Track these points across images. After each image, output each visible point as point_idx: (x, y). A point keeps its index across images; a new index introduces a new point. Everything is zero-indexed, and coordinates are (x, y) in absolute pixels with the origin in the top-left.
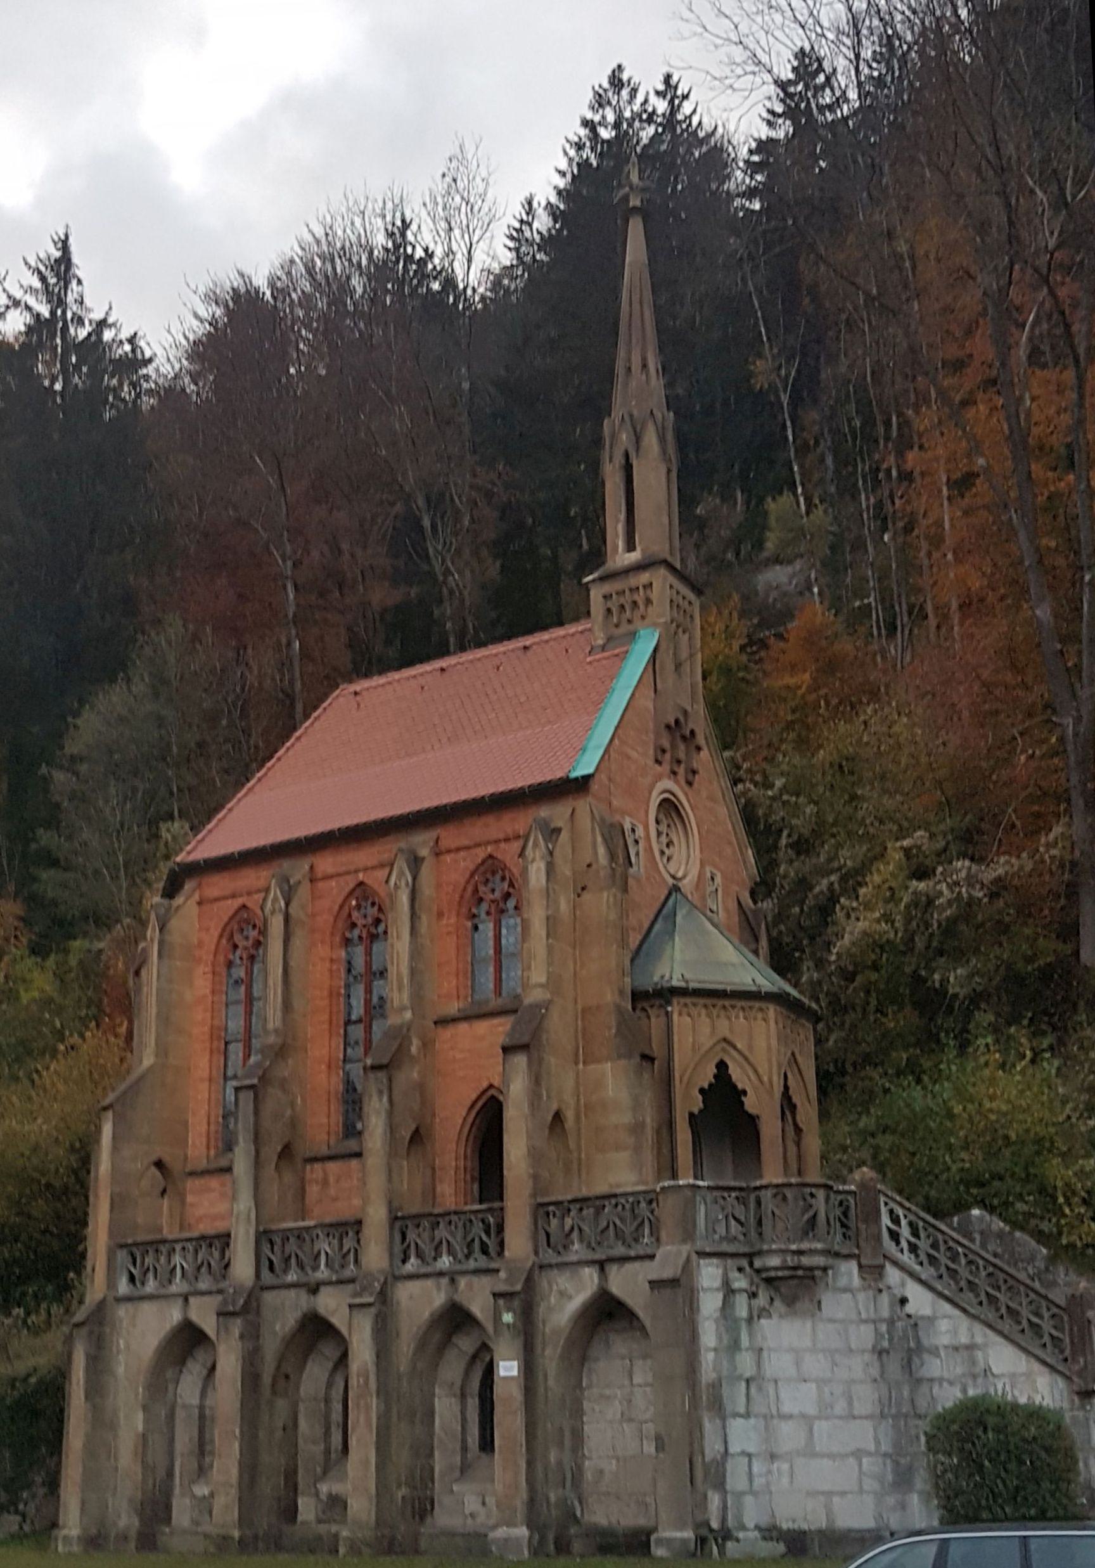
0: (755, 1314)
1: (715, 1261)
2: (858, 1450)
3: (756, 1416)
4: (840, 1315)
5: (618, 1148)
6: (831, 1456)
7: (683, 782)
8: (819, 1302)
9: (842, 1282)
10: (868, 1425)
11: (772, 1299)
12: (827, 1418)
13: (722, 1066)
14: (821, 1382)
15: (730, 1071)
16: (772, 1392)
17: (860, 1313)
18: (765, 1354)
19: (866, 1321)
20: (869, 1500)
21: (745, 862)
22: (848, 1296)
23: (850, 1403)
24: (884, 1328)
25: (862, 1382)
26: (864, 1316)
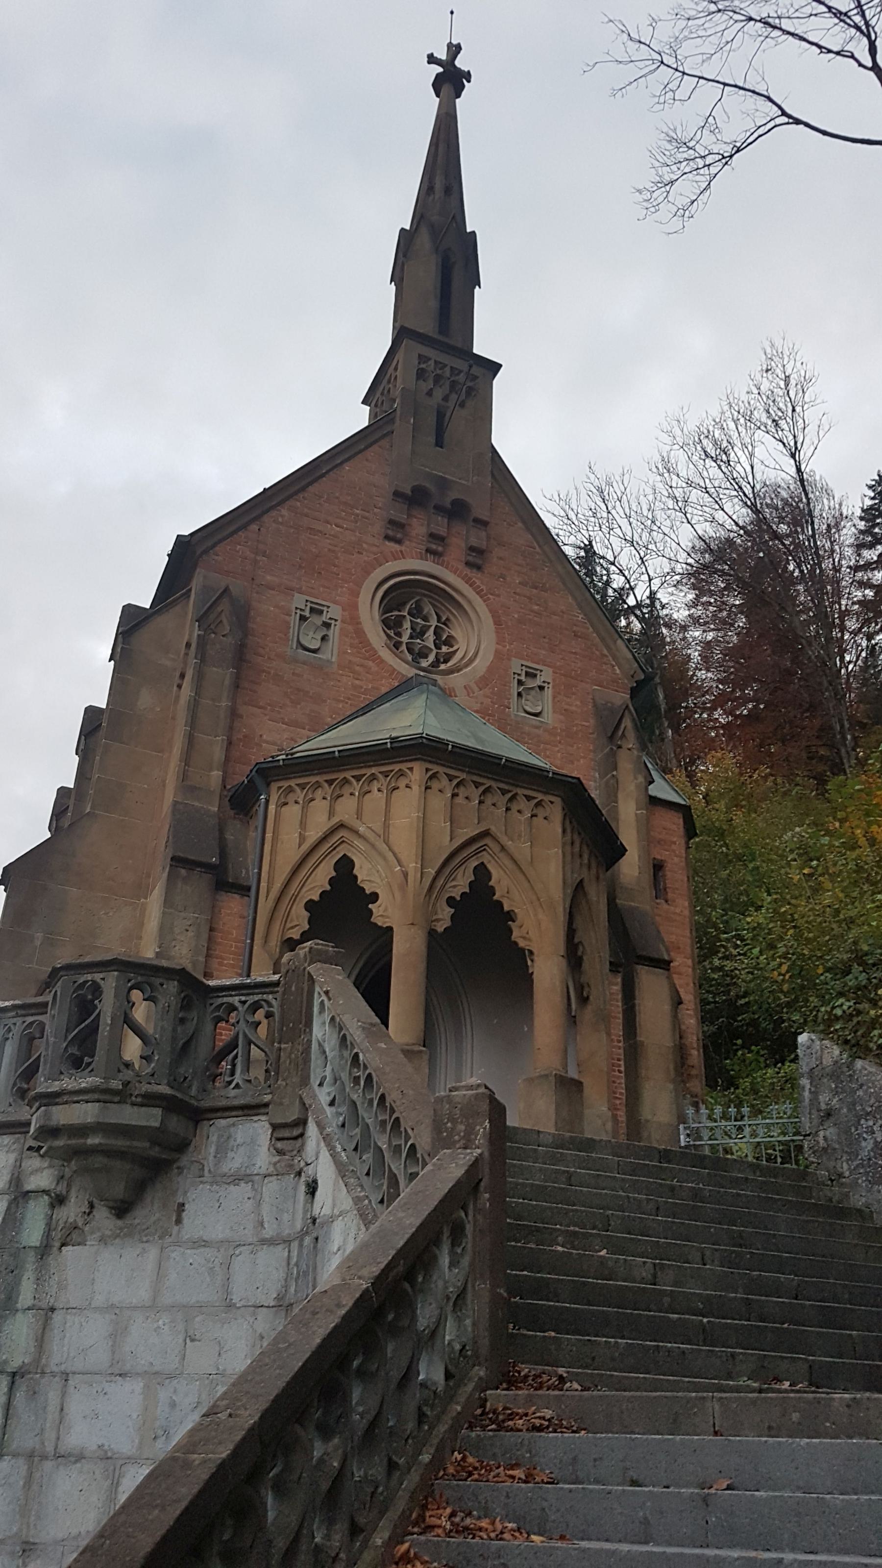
0: (57, 1235)
3: (15, 1455)
4: (218, 1231)
9: (234, 1163)
11: (92, 1206)
13: (345, 866)
15: (355, 872)
16: (53, 1397)
17: (262, 1224)
18: (57, 1317)
19: (270, 1242)
21: (614, 658)
22: (245, 1189)
26: (269, 1231)
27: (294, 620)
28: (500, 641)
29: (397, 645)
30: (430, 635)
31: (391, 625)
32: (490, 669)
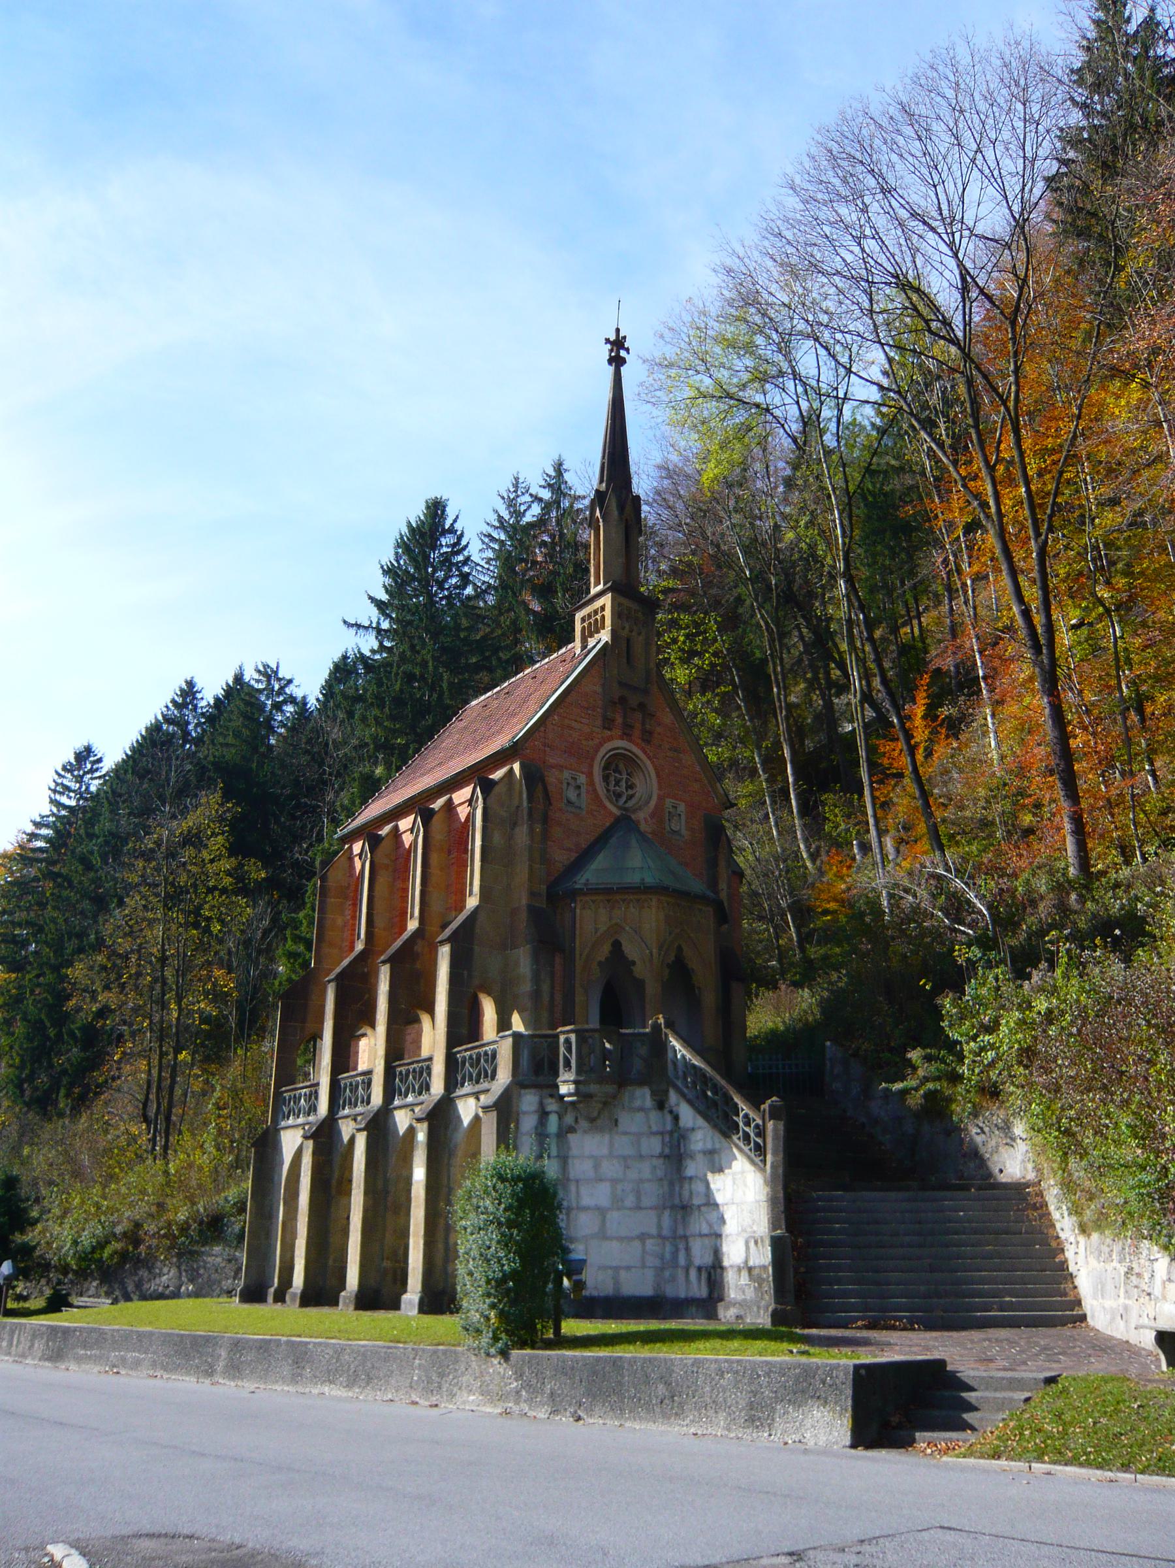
1: (533, 1091)
2: (643, 1234)
4: (634, 1129)
6: (620, 1239)
7: (639, 741)
8: (616, 1121)
9: (638, 1103)
10: (653, 1214)
12: (618, 1209)
13: (617, 945)
14: (614, 1182)
15: (624, 948)
17: (650, 1127)
18: (570, 1161)
20: (650, 1274)
23: (639, 1198)
24: (667, 1139)
25: (649, 1180)
26: (654, 1129)
27: (565, 785)
28: (660, 788)
29: (608, 790)
30: (623, 784)
31: (606, 778)
32: (656, 806)
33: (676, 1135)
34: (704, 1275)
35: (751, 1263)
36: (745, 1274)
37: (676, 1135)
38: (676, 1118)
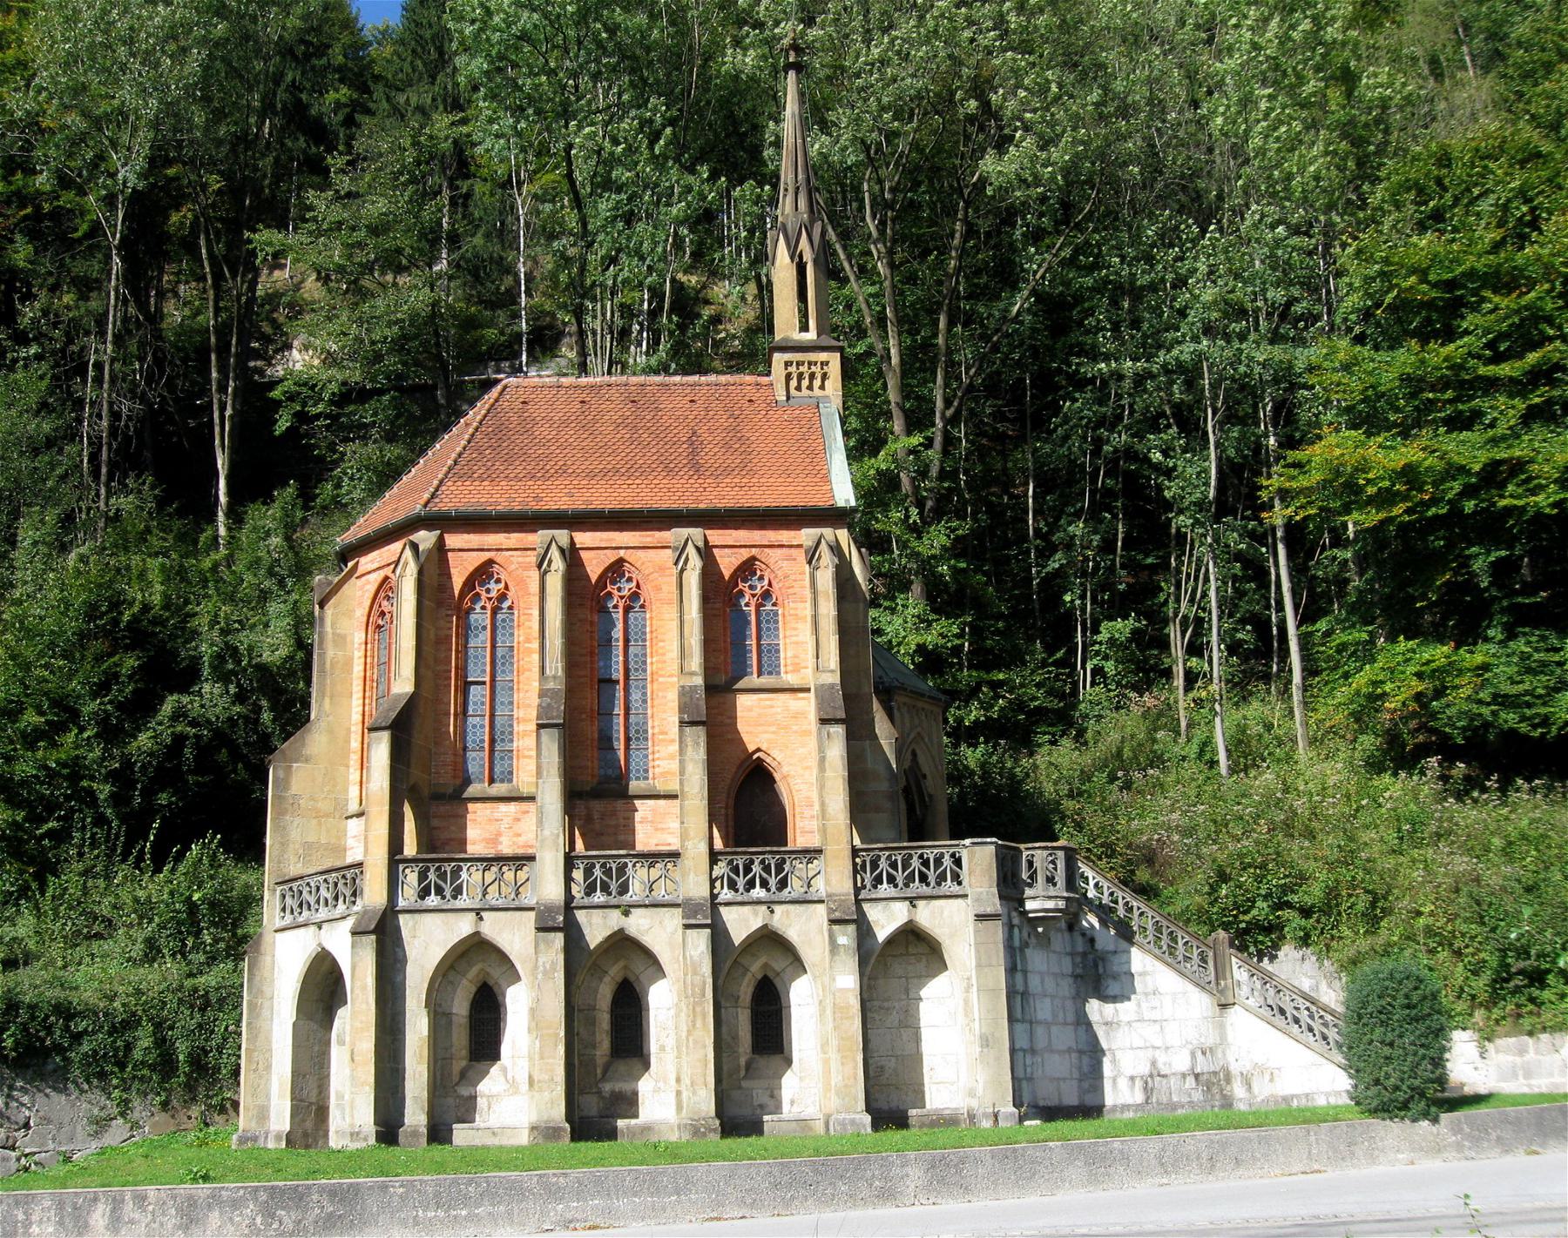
5: (878, 810)
24: (1078, 959)
33: (1091, 957)
34: (1139, 1084)
35: (1198, 1070)
36: (1191, 1081)
37: (1091, 957)
38: (1092, 941)
